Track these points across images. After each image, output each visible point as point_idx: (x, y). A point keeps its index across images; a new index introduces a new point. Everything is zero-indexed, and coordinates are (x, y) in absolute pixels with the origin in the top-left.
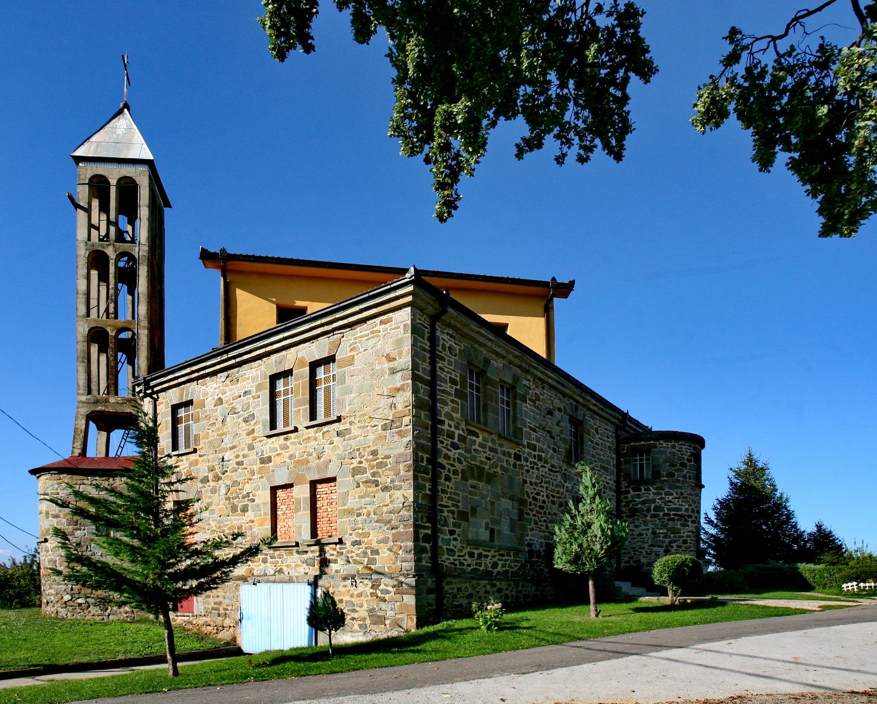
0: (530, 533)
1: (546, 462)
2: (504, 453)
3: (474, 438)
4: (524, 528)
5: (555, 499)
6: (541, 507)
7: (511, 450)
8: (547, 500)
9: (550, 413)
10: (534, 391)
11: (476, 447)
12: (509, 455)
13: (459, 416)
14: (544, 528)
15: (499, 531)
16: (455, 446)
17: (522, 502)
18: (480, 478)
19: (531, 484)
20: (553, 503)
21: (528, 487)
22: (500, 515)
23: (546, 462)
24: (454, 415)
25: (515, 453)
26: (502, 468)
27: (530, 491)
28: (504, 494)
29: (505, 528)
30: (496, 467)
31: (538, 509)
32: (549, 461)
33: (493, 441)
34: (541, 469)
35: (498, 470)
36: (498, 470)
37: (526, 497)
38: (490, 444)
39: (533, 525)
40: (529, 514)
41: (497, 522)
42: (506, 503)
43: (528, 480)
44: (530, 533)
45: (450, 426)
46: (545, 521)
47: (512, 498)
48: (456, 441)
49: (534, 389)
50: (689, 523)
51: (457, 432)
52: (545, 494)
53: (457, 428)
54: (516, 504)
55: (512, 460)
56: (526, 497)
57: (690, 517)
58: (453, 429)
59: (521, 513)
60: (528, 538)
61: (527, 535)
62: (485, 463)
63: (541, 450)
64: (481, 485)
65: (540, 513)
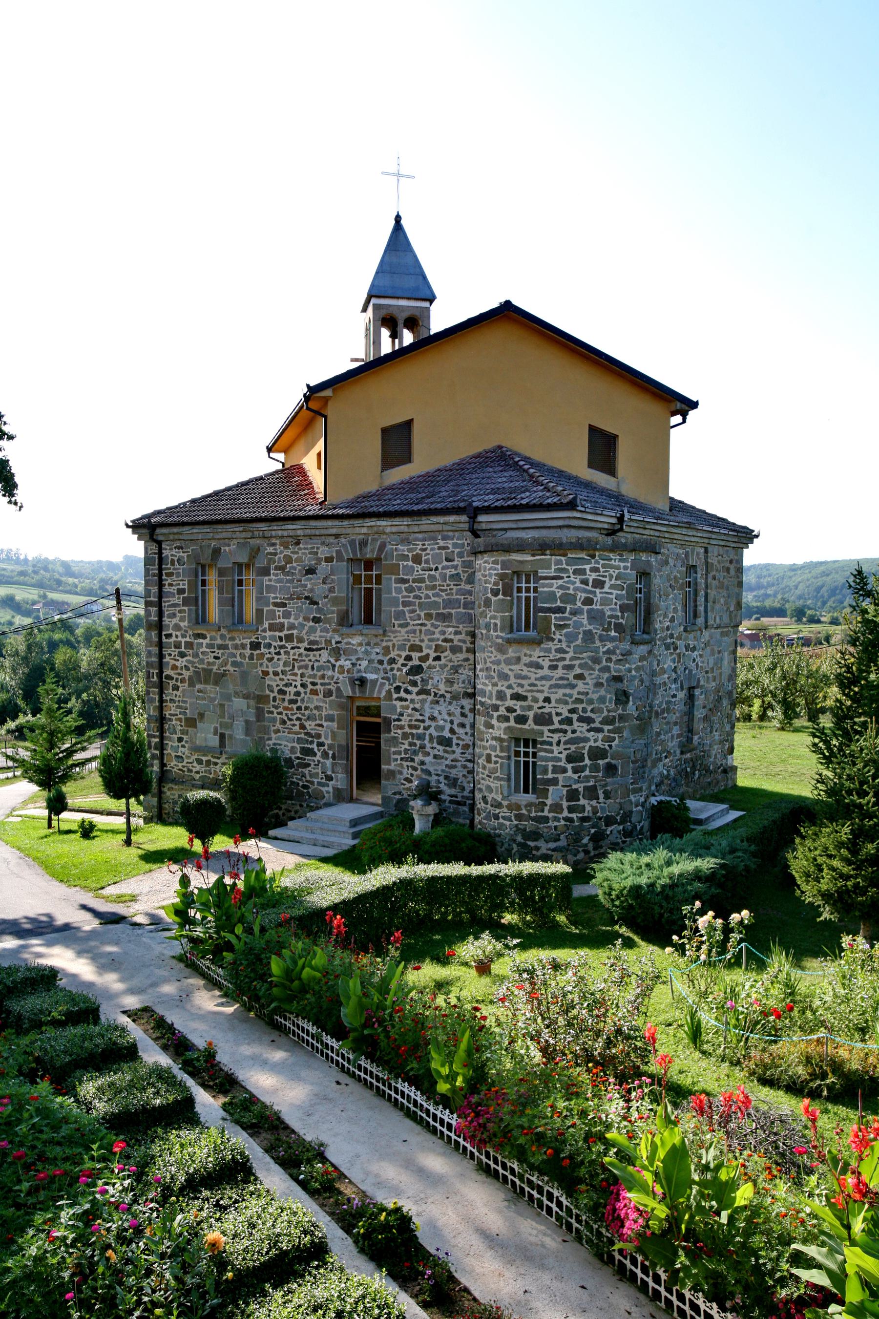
0: (273, 736)
1: (300, 640)
2: (236, 647)
3: (201, 641)
4: (266, 730)
5: (318, 687)
6: (292, 702)
7: (244, 641)
8: (302, 690)
9: (311, 571)
10: (282, 552)
11: (204, 649)
12: (243, 646)
13: (186, 623)
14: (297, 728)
15: (231, 736)
16: (182, 655)
17: (262, 699)
18: (206, 682)
19: (276, 674)
20: (315, 692)
21: (271, 680)
22: (232, 717)
23: (300, 640)
24: (182, 624)
25: (251, 643)
26: (234, 664)
27: (274, 684)
28: (237, 694)
29: (239, 733)
30: (226, 665)
31: (286, 704)
32: (306, 637)
33: (223, 637)
34: (292, 652)
35: (229, 667)
36: (229, 667)
37: (267, 692)
38: (219, 642)
39: (278, 726)
40: (272, 713)
41: (229, 726)
42: (239, 703)
43: (271, 670)
44: (273, 736)
45: (177, 636)
46: (298, 719)
47: (246, 697)
48: (183, 649)
49: (281, 552)
50: (494, 722)
51: (183, 640)
52: (298, 684)
53: (183, 636)
54: (252, 703)
55: (248, 652)
56: (267, 692)
57: (496, 708)
58: (180, 639)
59: (260, 714)
60: (271, 742)
61: (270, 739)
62: (214, 664)
63: (292, 627)
64: (208, 687)
65: (292, 709)
